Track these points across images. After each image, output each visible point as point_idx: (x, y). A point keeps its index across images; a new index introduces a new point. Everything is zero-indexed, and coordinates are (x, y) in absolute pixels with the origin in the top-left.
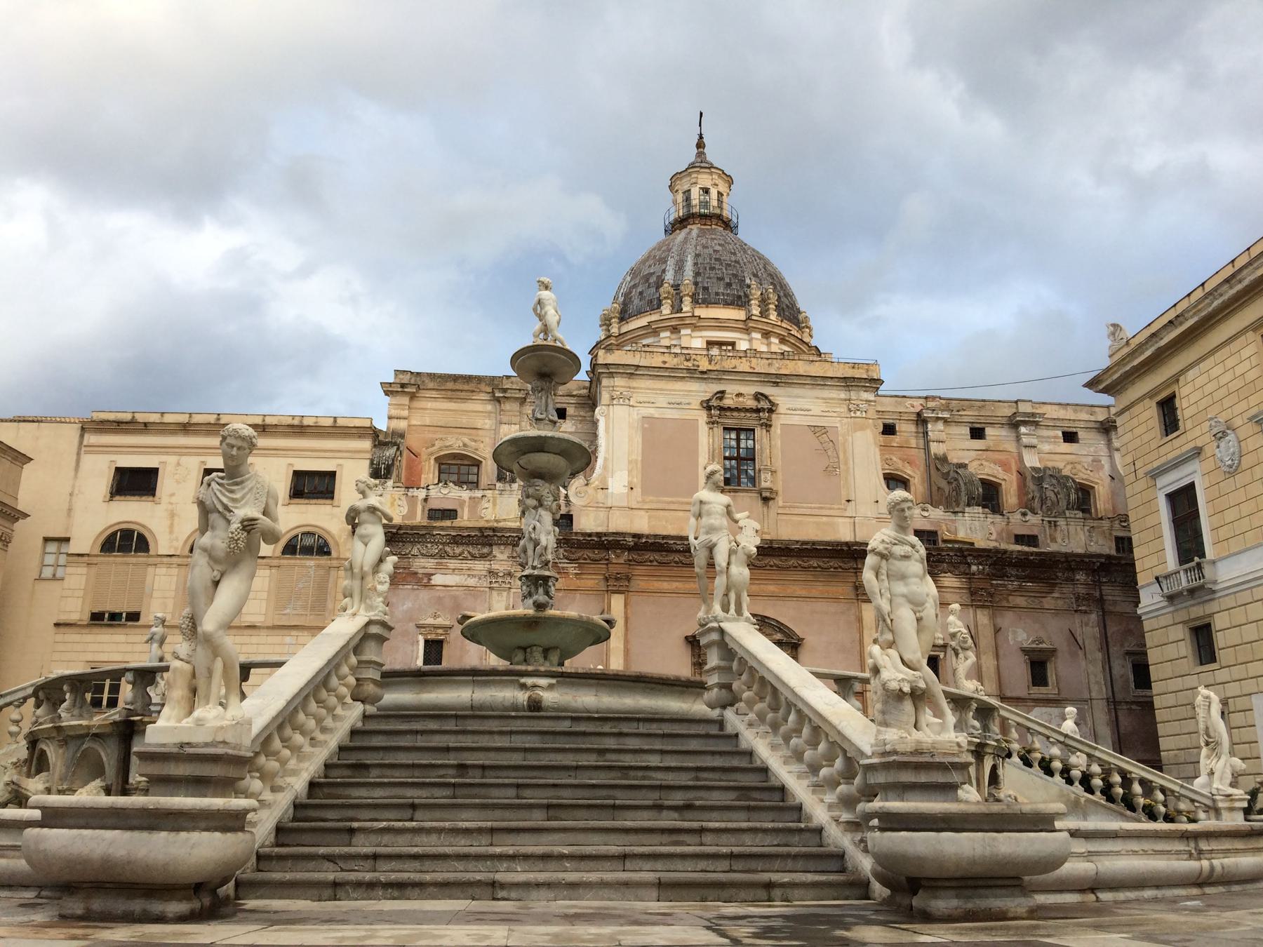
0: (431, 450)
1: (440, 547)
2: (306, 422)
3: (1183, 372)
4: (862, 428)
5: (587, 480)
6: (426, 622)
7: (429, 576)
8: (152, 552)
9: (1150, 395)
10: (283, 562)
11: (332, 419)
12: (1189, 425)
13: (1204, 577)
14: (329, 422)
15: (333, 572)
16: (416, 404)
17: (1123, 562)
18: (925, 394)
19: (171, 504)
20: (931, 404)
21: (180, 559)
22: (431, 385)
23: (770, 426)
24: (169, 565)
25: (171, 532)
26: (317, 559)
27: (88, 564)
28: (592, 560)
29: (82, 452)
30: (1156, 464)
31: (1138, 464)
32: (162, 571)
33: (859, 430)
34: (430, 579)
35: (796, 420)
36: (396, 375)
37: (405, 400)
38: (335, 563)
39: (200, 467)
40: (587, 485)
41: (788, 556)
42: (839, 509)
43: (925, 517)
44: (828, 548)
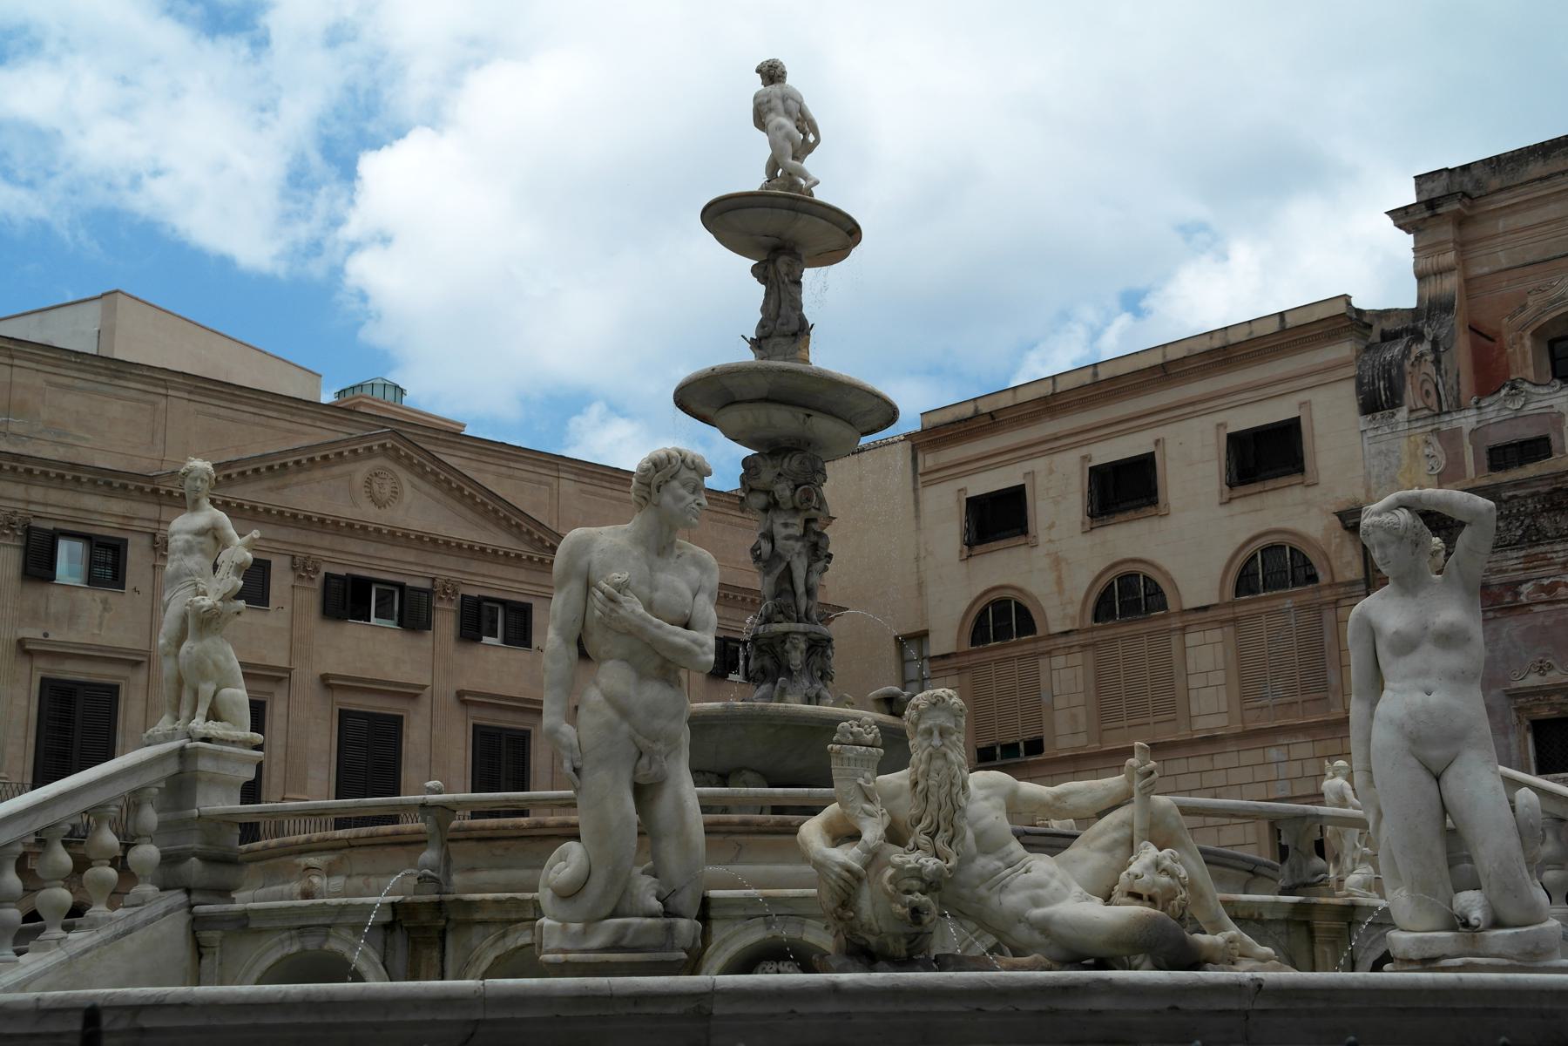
0: (1522, 317)
1: (1527, 522)
2: (1233, 339)
6: (1521, 684)
7: (1513, 587)
8: (1040, 633)
10: (1241, 610)
11: (1277, 319)
14: (1274, 326)
15: (1328, 616)
16: (1473, 231)
19: (1050, 541)
21: (1082, 637)
22: (1495, 183)
24: (1068, 649)
25: (1061, 592)
26: (1295, 594)
27: (959, 669)
29: (920, 485)
32: (1059, 661)
34: (1517, 594)
36: (1418, 186)
37: (1447, 232)
38: (1328, 595)
39: (1083, 468)
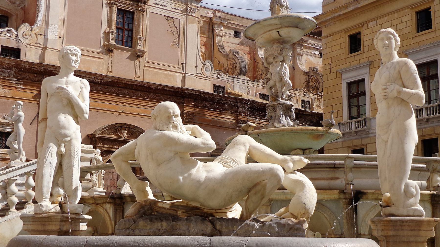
3: (367, 22)
4: (193, 22)
5: (31, 28)
9: (346, 31)
12: (366, 49)
13: (365, 125)
17: (305, 113)
18: (215, 7)
20: (218, 14)
23: (144, 12)
28: (32, 81)
30: (344, 67)
31: (332, 65)
33: (191, 23)
35: (158, 11)
40: (31, 30)
41: (149, 92)
42: (177, 68)
43: (219, 78)
44: (172, 90)
